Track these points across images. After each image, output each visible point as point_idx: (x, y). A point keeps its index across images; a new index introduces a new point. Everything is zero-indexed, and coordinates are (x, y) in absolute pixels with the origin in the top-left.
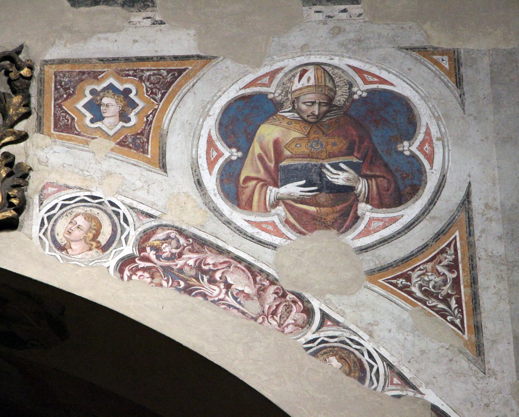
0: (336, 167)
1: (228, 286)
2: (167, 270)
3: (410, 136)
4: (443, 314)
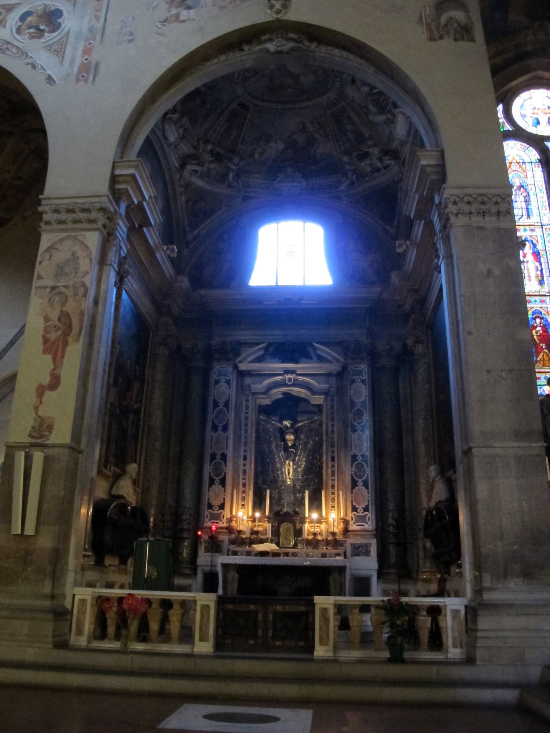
0: (43, 25)
1: (11, 51)
3: (60, 18)
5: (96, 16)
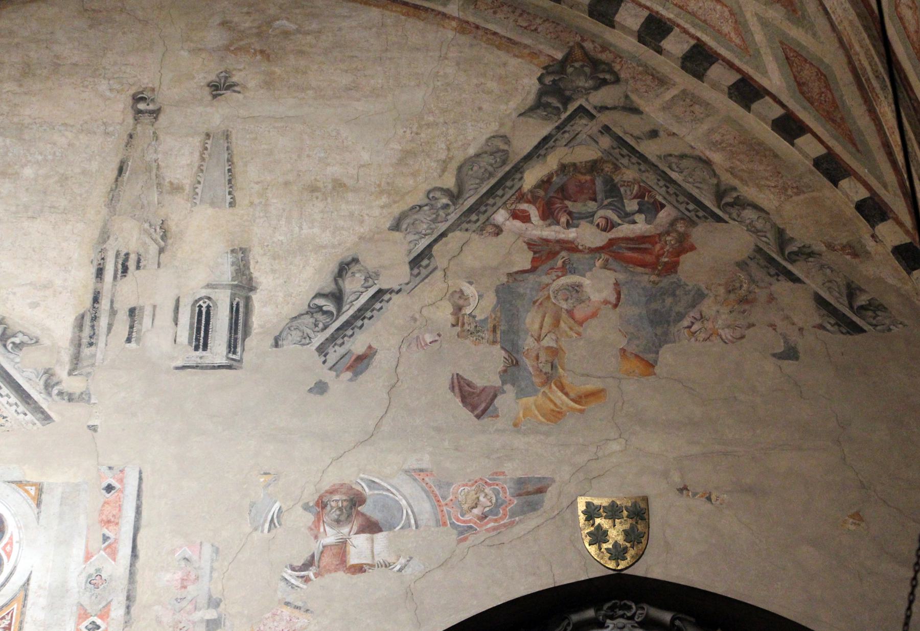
5: (105, 538)
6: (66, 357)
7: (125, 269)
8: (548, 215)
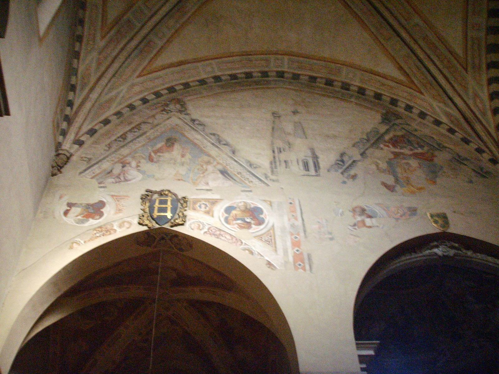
2: (214, 234)
4: (269, 244)
5: (293, 216)
6: (269, 171)
7: (280, 151)
8: (394, 146)
